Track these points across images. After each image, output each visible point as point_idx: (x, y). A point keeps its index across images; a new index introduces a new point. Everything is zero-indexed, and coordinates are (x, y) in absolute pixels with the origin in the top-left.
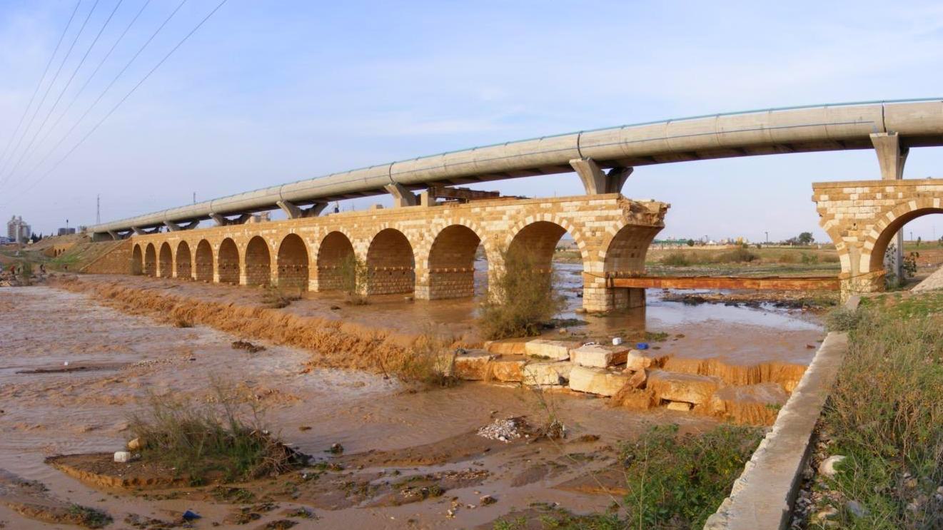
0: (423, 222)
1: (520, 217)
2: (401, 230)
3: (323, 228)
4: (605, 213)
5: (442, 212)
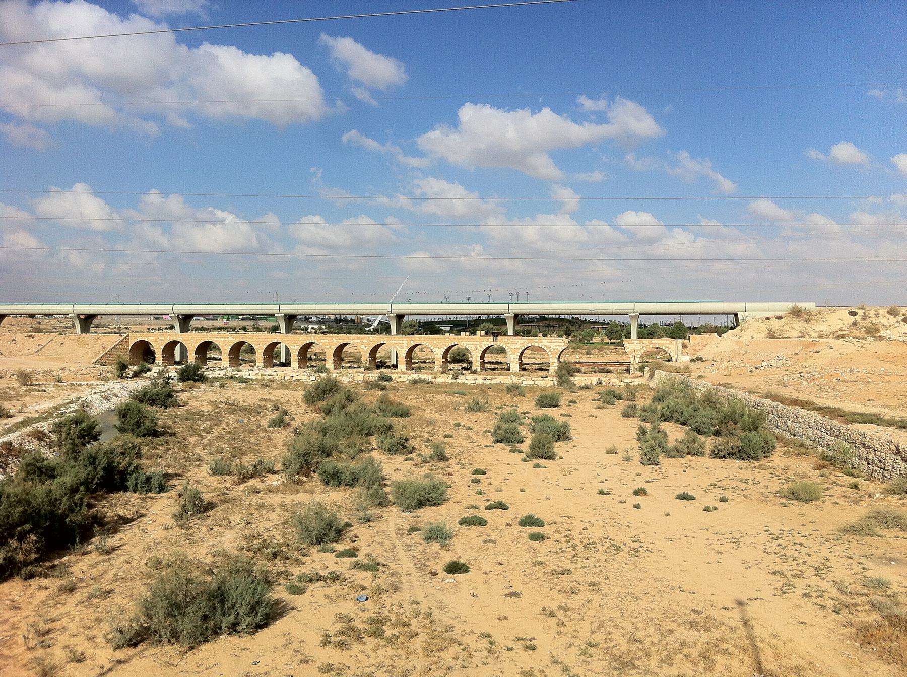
0: (478, 343)
4: (558, 344)
5: (488, 339)
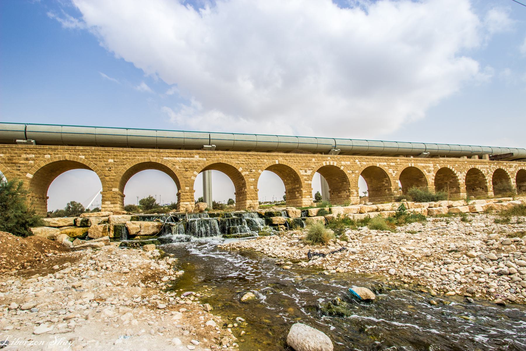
0: (488, 166)
1: (517, 167)
2: (479, 169)
3: (436, 165)
5: (494, 163)
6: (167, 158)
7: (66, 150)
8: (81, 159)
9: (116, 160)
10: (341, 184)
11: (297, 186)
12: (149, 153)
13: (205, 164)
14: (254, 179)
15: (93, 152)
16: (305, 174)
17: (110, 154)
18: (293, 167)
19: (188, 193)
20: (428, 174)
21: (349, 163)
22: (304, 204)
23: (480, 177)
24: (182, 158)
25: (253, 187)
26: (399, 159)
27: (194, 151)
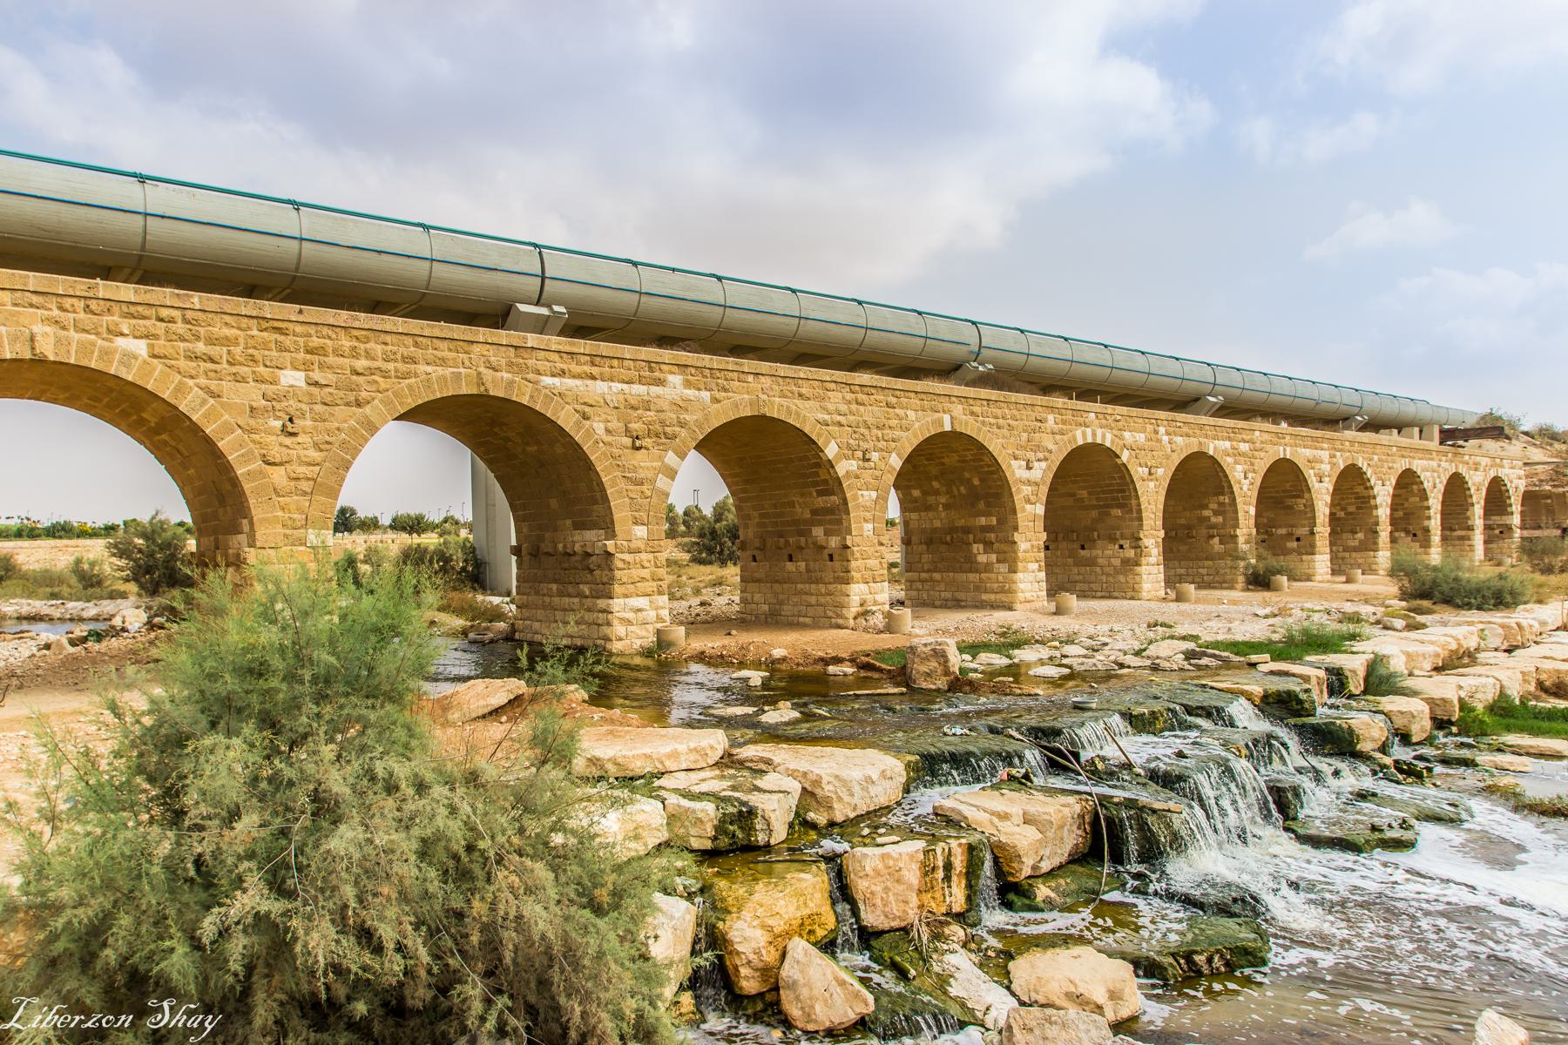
0: (1434, 464)
3: (1334, 456)
6: (556, 381)
7: (35, 299)
8: (129, 356)
9: (317, 376)
10: (1094, 514)
11: (983, 521)
12: (476, 349)
13: (706, 418)
14: (874, 494)
15: (196, 322)
16: (1025, 474)
17: (287, 341)
18: (994, 445)
19: (644, 556)
20: (1317, 485)
21: (1141, 437)
22: (1021, 596)
23: (1412, 499)
24: (620, 386)
25: (870, 526)
26: (1260, 429)
27: (667, 355)
